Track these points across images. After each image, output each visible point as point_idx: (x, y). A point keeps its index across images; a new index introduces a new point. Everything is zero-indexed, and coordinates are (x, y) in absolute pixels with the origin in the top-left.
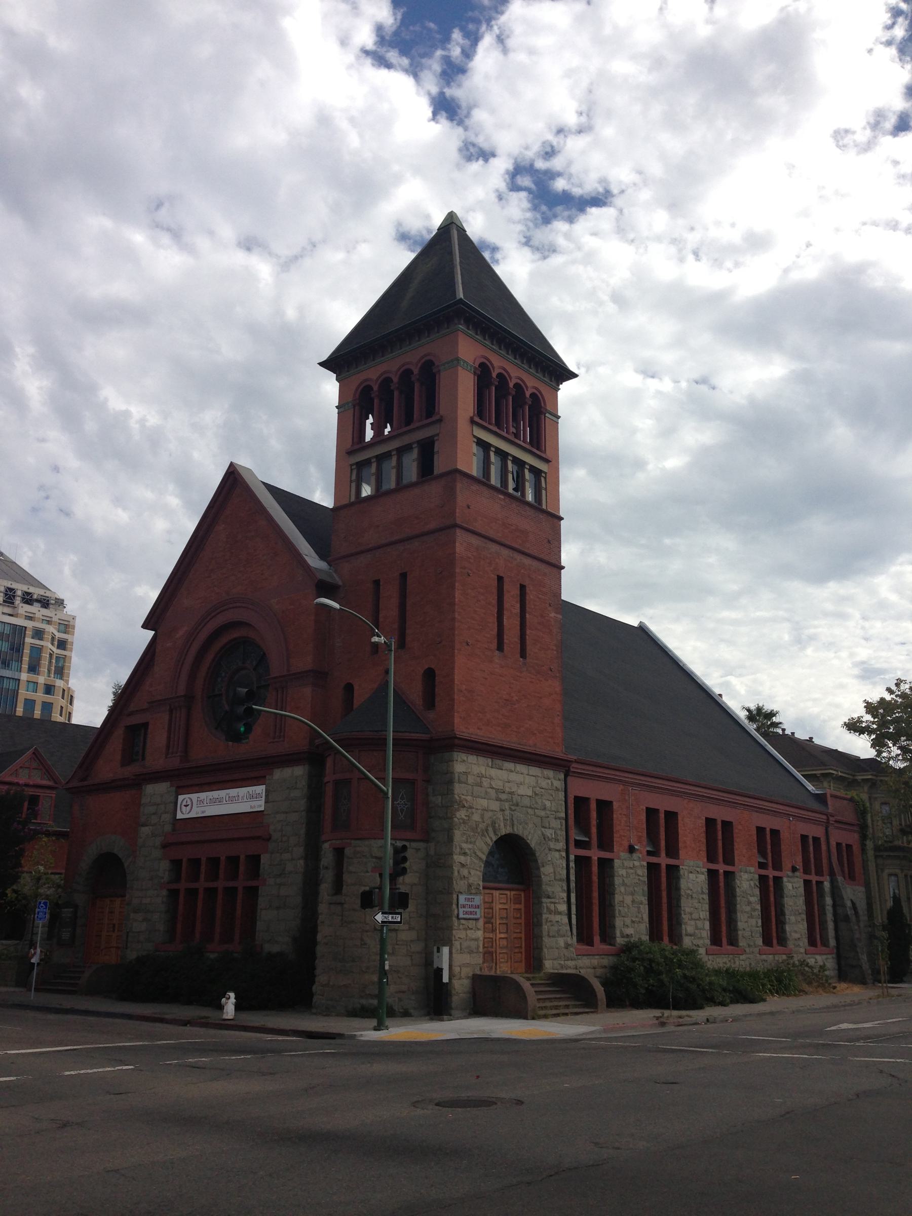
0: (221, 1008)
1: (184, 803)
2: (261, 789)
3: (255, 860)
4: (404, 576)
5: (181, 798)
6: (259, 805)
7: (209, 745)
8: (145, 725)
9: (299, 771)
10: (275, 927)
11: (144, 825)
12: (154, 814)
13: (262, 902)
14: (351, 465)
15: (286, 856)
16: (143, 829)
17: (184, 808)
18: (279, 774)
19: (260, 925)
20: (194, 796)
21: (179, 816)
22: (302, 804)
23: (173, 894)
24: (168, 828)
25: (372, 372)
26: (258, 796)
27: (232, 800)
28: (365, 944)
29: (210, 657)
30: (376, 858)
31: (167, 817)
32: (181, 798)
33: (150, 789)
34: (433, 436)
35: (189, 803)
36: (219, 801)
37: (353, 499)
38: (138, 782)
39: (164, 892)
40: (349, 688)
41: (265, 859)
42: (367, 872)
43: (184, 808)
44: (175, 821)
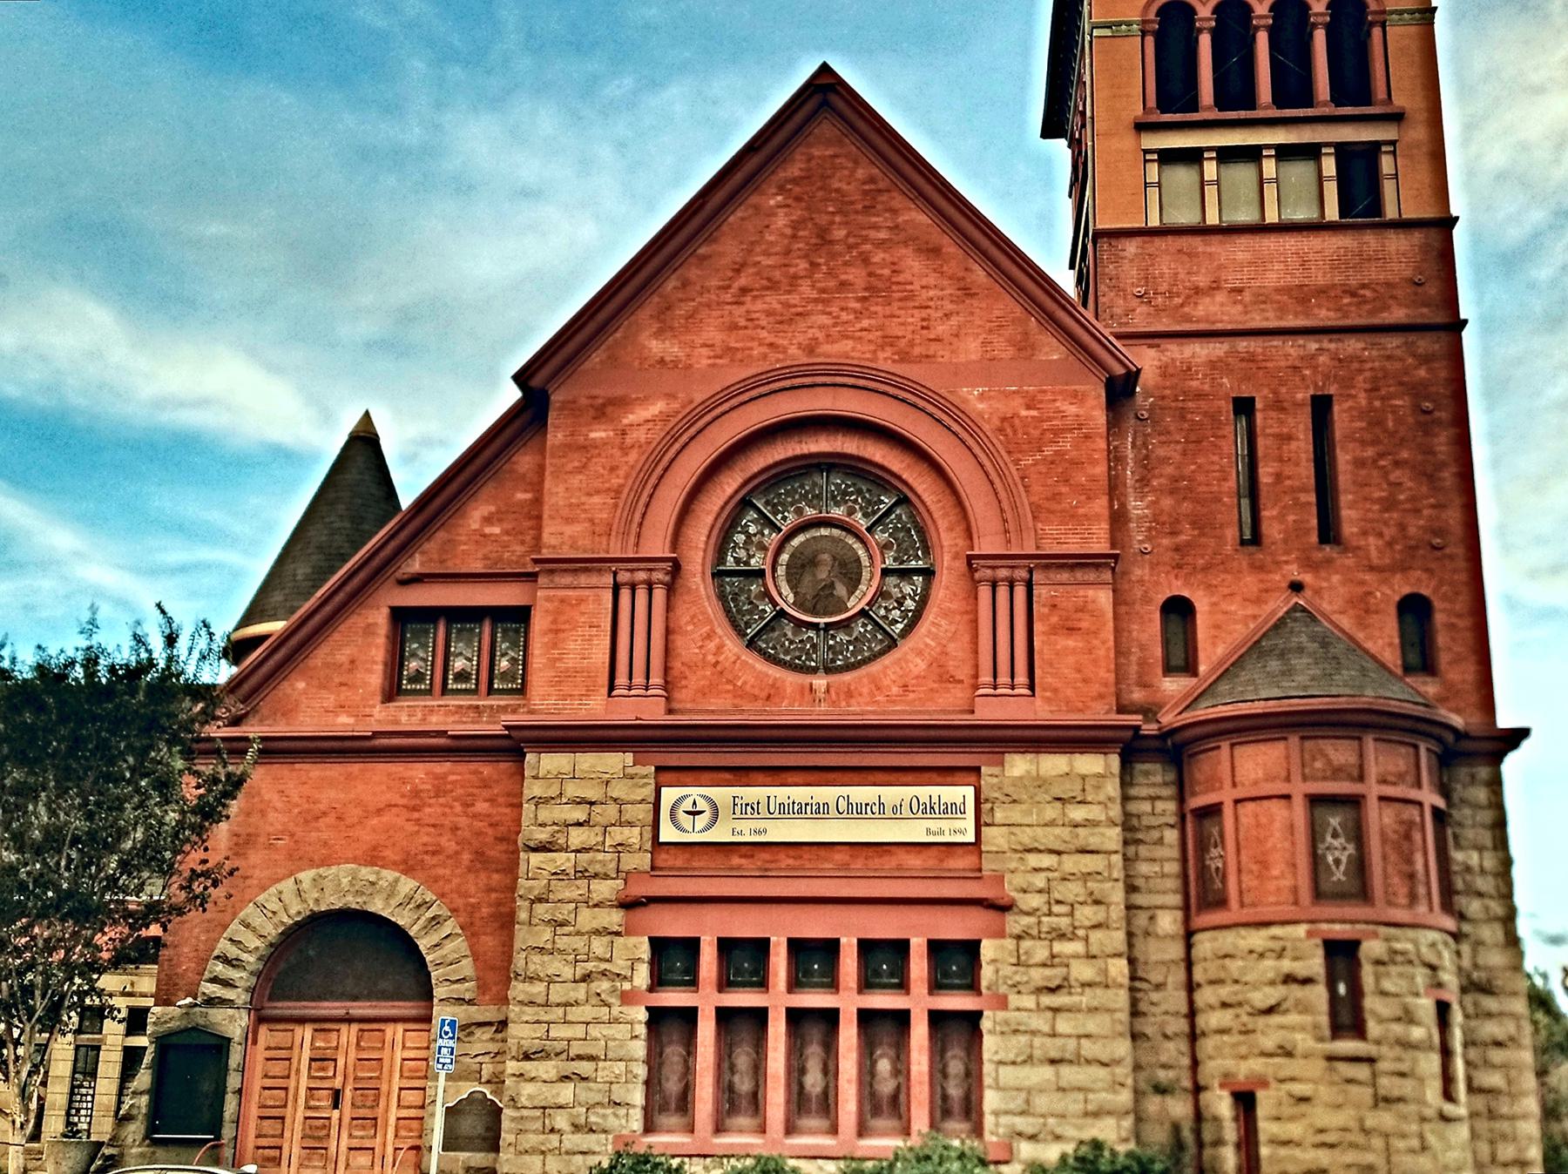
1: (687, 805)
2: (962, 794)
5: (669, 795)
8: (519, 616)
9: (1090, 764)
12: (579, 824)
14: (1146, 152)
18: (1019, 765)
22: (1112, 837)
26: (952, 810)
27: (858, 811)
29: (729, 484)
32: (669, 795)
35: (702, 805)
38: (512, 748)
40: (1179, 610)
42: (1417, 995)
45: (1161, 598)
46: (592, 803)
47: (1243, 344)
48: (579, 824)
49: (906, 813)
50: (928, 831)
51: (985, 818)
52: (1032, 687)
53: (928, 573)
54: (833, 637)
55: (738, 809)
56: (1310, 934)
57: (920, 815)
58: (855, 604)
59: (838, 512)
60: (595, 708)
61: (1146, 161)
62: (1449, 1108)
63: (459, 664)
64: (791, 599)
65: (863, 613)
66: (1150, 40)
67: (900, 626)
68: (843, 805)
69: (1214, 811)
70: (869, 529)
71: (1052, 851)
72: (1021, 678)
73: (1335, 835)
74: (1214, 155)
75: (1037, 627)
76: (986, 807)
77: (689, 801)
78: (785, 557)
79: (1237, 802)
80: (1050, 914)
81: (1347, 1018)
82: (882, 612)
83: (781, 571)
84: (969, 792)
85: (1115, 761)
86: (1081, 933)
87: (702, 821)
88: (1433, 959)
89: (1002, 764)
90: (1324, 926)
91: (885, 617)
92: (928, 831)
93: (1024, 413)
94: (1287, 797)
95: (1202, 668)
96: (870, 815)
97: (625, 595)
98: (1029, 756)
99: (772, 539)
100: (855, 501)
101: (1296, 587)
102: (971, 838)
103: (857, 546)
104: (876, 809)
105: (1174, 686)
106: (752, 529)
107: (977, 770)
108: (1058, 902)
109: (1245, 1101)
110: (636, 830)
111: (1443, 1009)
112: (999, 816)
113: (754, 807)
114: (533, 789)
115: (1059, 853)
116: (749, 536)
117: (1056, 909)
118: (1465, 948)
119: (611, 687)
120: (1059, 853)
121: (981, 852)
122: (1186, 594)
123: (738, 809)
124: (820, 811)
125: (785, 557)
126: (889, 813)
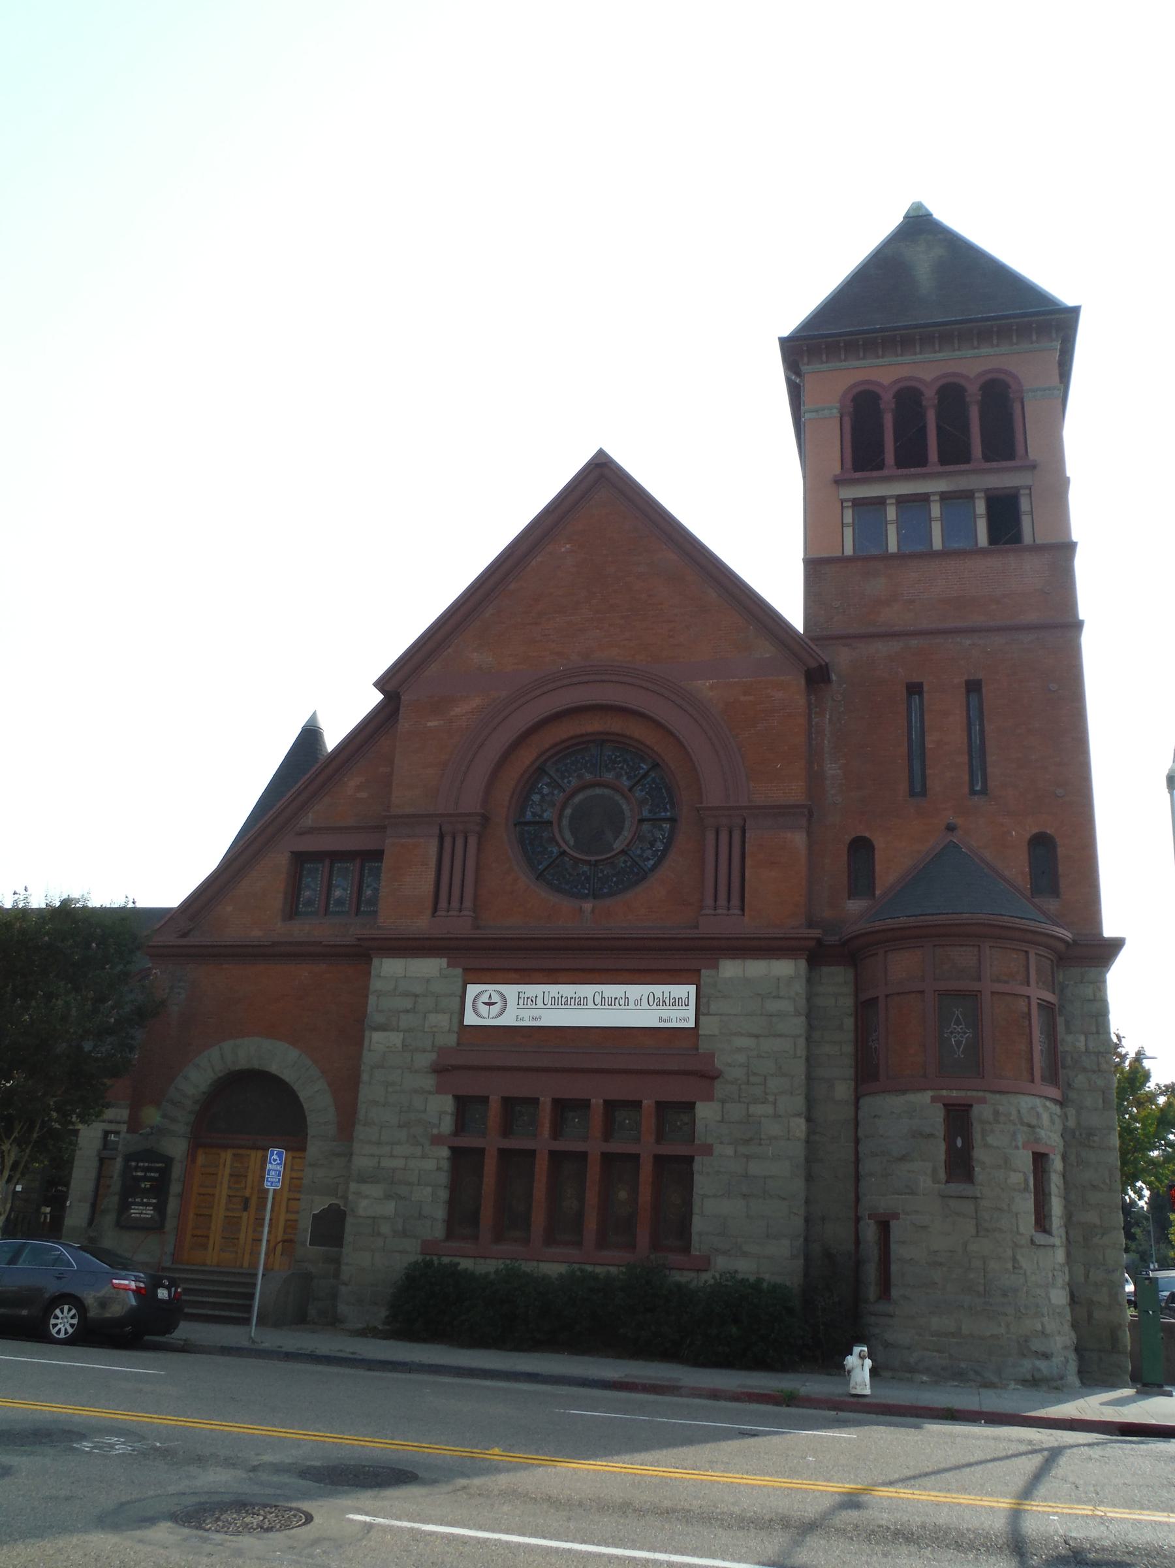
0: (843, 1372)
2: (687, 991)
3: (675, 1113)
4: (973, 687)
6: (684, 1017)
7: (524, 902)
9: (784, 968)
10: (745, 1227)
11: (382, 1028)
12: (407, 1011)
13: (703, 1184)
14: (842, 501)
15: (758, 1109)
16: (377, 1036)
17: (483, 1009)
18: (730, 969)
19: (698, 1225)
20: (511, 991)
21: (470, 1019)
22: (797, 1025)
23: (464, 1161)
24: (452, 1040)
25: (886, 372)
26: (676, 1002)
27: (609, 1003)
28: (1021, 1268)
29: (527, 757)
30: (1029, 1126)
31: (441, 1021)
32: (472, 990)
33: (389, 968)
34: (1017, 489)
36: (581, 1002)
37: (849, 551)
39: (445, 1152)
40: (861, 848)
41: (705, 1112)
43: (483, 1009)
44: (463, 1028)
45: (848, 839)
46: (416, 996)
47: (914, 642)
48: (407, 1011)
49: (645, 1005)
50: (660, 1019)
51: (702, 1009)
52: (743, 909)
53: (673, 820)
54: (602, 871)
55: (521, 1001)
56: (934, 1099)
57: (655, 1007)
58: (618, 846)
59: (609, 776)
60: (421, 924)
61: (842, 507)
62: (1041, 1238)
63: (338, 893)
64: (572, 842)
65: (623, 852)
66: (847, 419)
67: (652, 862)
68: (598, 999)
69: (875, 1000)
70: (630, 790)
71: (751, 1035)
72: (735, 901)
73: (958, 1023)
74: (894, 501)
75: (748, 862)
76: (703, 1000)
77: (486, 995)
78: (568, 811)
79: (887, 996)
80: (748, 1083)
81: (960, 1165)
82: (639, 852)
83: (565, 822)
84: (692, 989)
85: (803, 964)
86: (771, 1098)
87: (495, 1009)
88: (1034, 1122)
89: (716, 967)
90: (944, 1093)
91: (640, 856)
92: (660, 1019)
93: (742, 698)
94: (922, 992)
95: (878, 892)
96: (618, 1006)
97: (448, 841)
98: (738, 962)
99: (559, 797)
100: (622, 768)
101: (951, 828)
102: (692, 1024)
103: (622, 802)
104: (622, 1002)
105: (855, 906)
106: (546, 790)
107: (699, 971)
108: (755, 1074)
109: (884, 1227)
110: (447, 1017)
111: (1040, 1159)
112: (713, 1007)
113: (533, 1000)
114: (376, 984)
115: (757, 1036)
116: (543, 796)
117: (753, 1079)
118: (1071, 1112)
119: (435, 909)
120: (757, 1036)
121: (698, 1035)
122: (867, 835)
123: (521, 1001)
124: (581, 1002)
125: (568, 811)
126: (632, 1005)
